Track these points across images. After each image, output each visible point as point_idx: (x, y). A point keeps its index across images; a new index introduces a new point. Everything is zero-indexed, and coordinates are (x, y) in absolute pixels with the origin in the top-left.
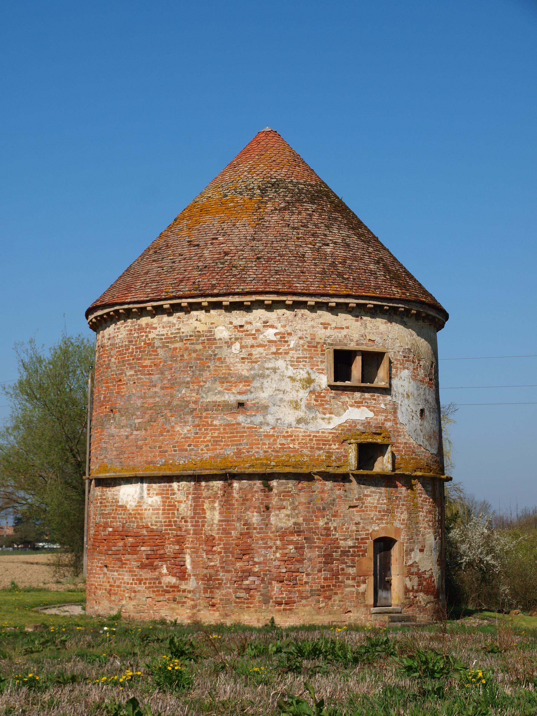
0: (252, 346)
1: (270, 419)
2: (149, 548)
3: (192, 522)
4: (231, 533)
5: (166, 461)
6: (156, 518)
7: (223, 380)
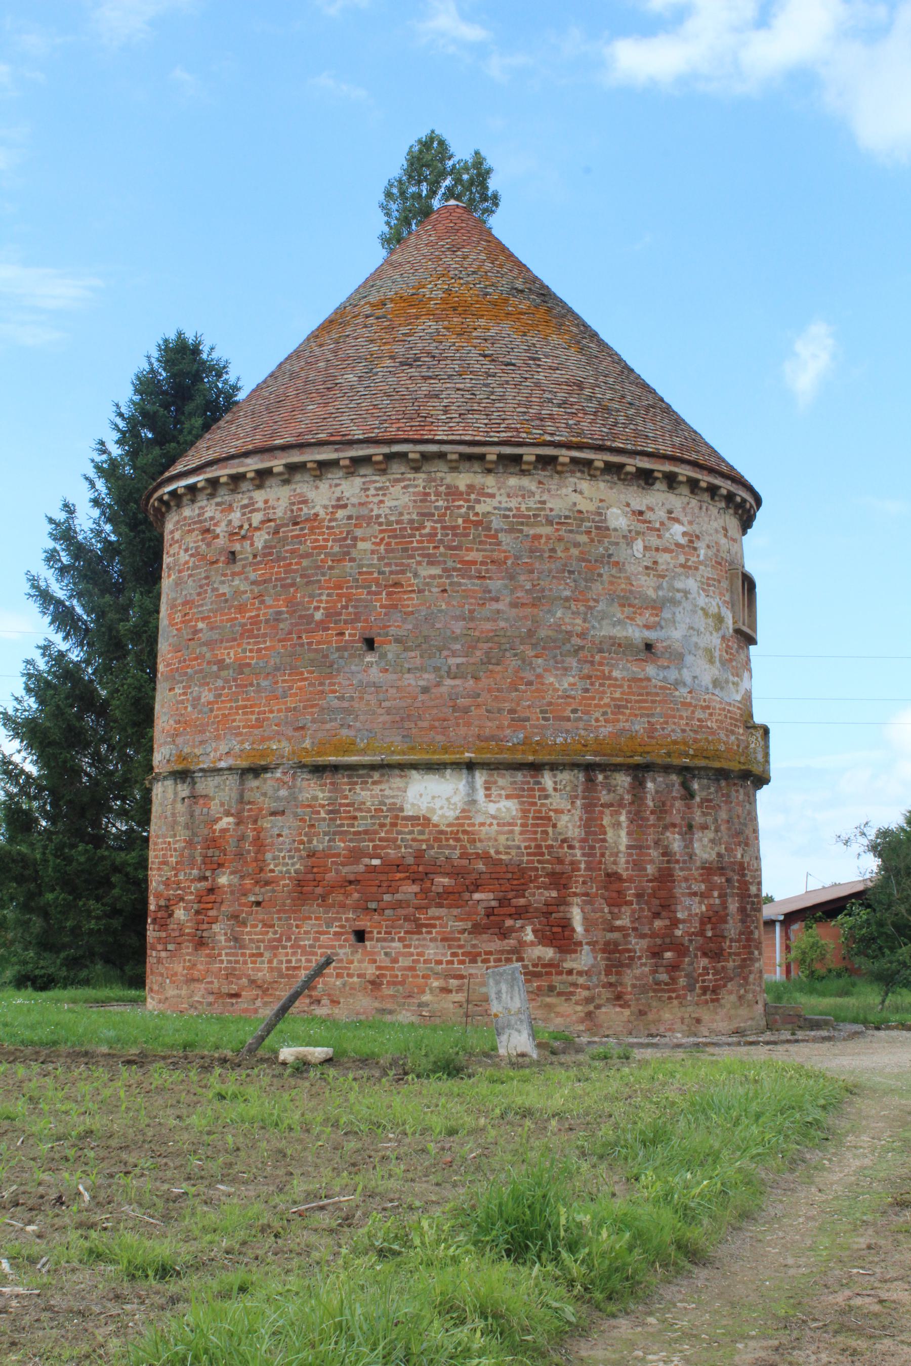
0: (657, 549)
1: (687, 675)
2: (491, 896)
3: (582, 848)
4: (645, 869)
5: (526, 737)
6: (507, 839)
7: (624, 602)
